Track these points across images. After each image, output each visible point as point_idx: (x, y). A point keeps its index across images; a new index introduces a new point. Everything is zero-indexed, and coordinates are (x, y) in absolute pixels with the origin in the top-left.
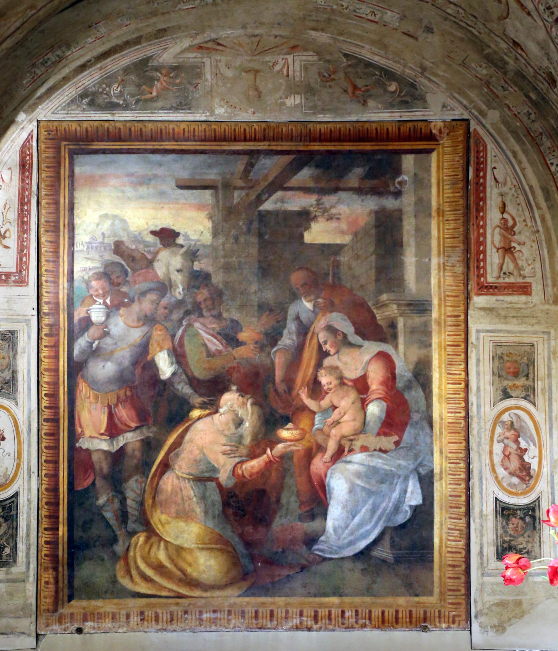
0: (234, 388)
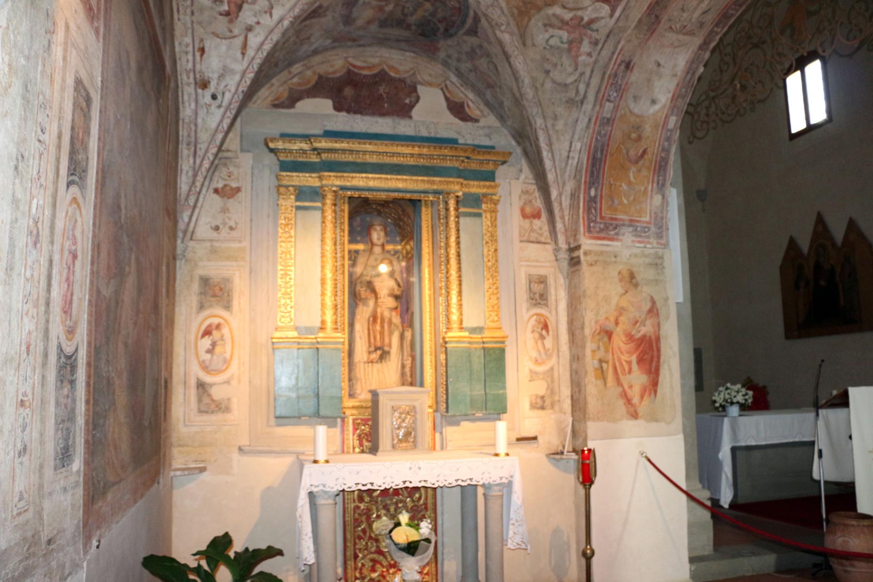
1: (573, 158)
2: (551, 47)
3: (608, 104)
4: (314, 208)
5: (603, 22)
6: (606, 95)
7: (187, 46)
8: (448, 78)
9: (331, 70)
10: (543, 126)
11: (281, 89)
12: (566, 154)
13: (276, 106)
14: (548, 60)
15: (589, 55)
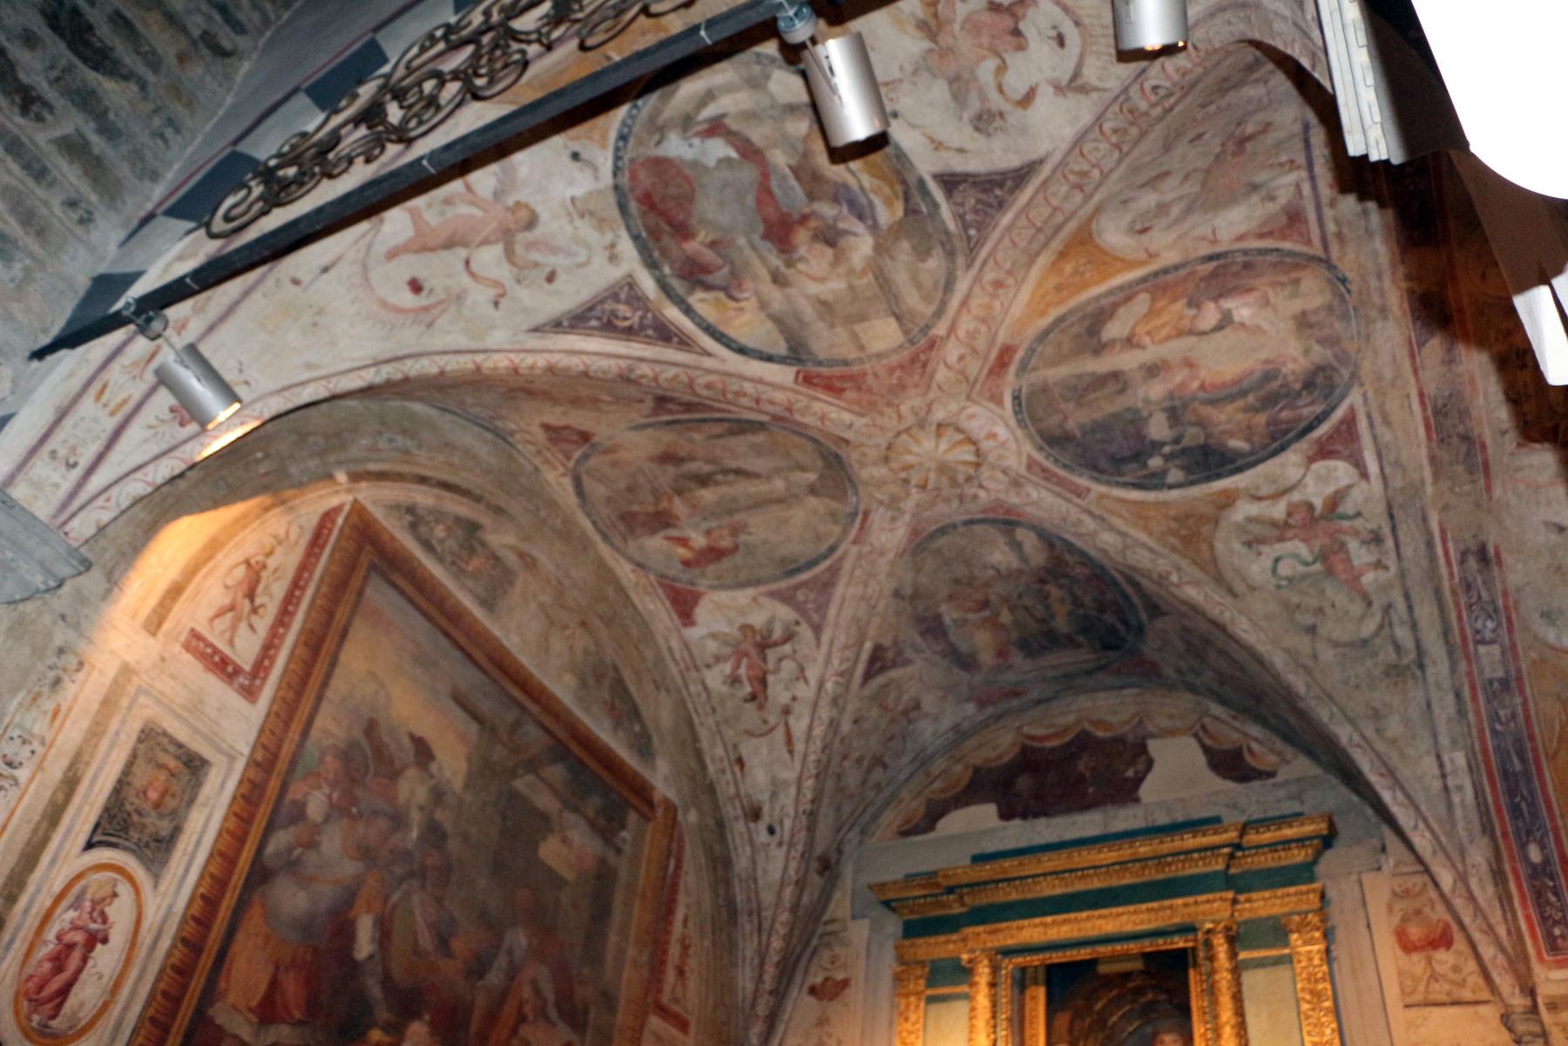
0: (427, 1017)
1: (1460, 788)
2: (1290, 579)
3: (1482, 649)
4: (959, 997)
5: (1357, 495)
6: (1469, 632)
7: (721, 760)
8: (1206, 713)
9: (994, 754)
10: (1356, 738)
11: (915, 804)
12: (1437, 785)
13: (905, 833)
14: (1298, 606)
15: (1379, 565)
